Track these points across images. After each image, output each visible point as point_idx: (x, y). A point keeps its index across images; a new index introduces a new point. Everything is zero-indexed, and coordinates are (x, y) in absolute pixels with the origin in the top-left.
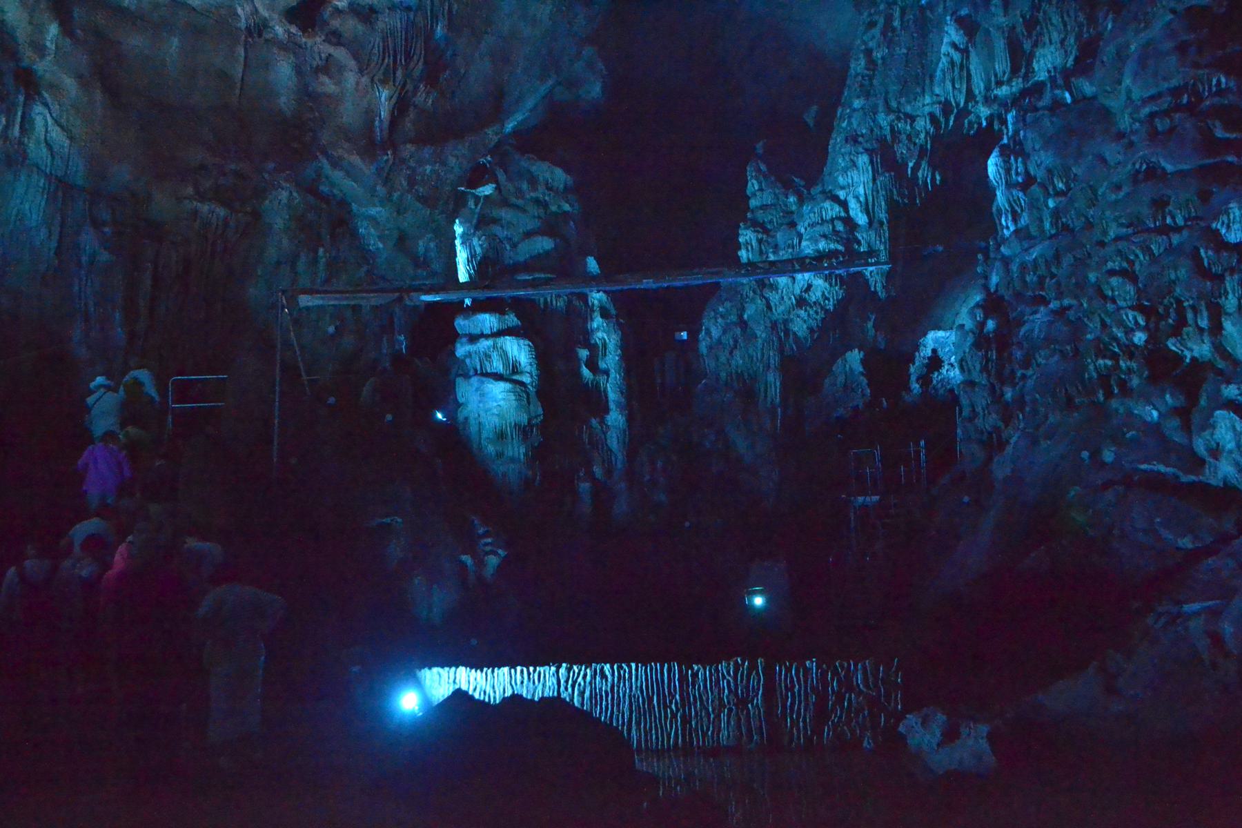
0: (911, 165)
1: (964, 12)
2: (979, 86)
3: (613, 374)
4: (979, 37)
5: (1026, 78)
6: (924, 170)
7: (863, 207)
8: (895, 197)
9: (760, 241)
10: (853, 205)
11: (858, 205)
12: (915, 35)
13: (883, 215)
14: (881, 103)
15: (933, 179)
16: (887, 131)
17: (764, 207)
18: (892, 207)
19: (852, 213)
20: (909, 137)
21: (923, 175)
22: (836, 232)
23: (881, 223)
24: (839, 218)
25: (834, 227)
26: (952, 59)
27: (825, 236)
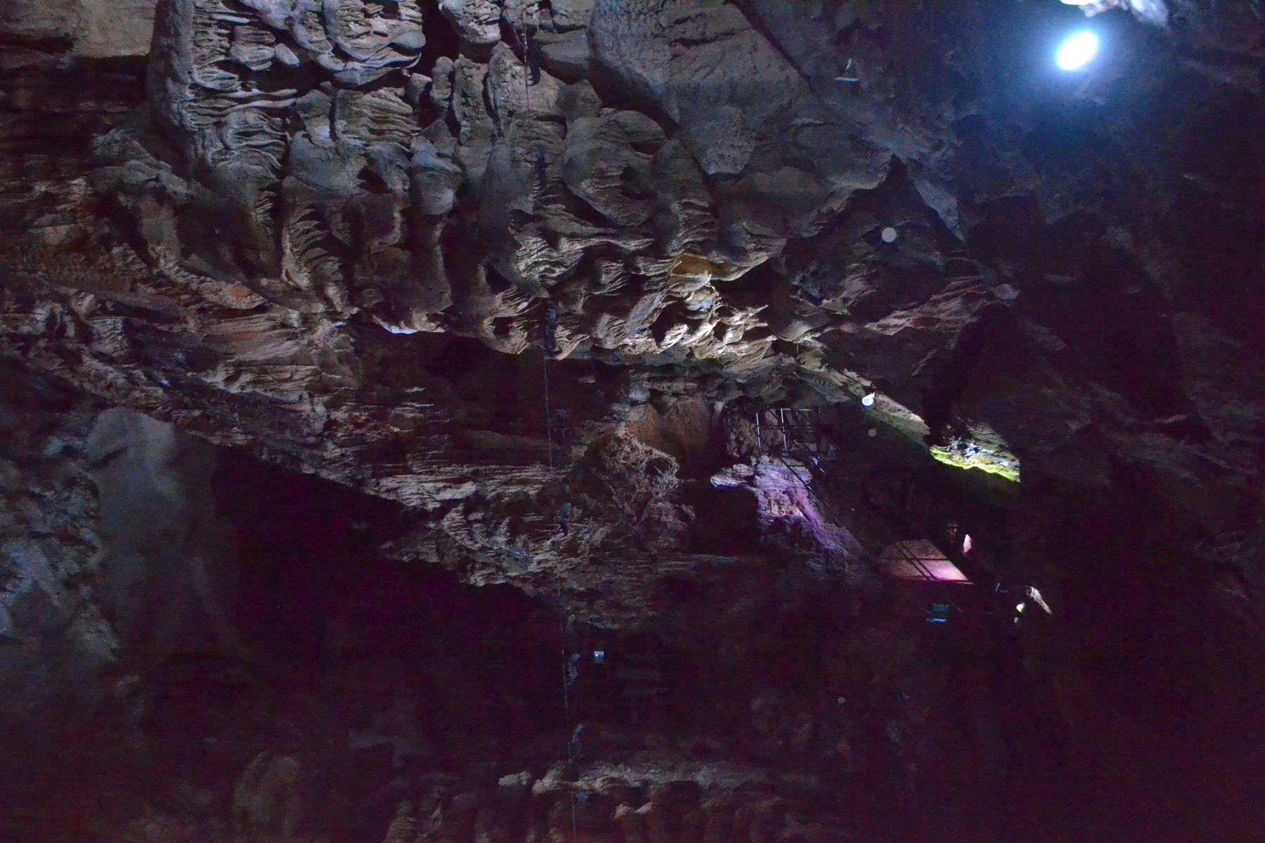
0: (396, 430)
2: (287, 348)
3: (649, 776)
6: (404, 410)
7: (452, 485)
8: (441, 452)
10: (447, 495)
11: (449, 490)
12: (213, 400)
13: (466, 470)
14: (307, 452)
15: (415, 397)
16: (350, 450)
19: (458, 496)
20: (358, 426)
21: (412, 412)
22: (483, 521)
24: (466, 513)
25: (477, 521)
26: (249, 383)
27: (489, 534)
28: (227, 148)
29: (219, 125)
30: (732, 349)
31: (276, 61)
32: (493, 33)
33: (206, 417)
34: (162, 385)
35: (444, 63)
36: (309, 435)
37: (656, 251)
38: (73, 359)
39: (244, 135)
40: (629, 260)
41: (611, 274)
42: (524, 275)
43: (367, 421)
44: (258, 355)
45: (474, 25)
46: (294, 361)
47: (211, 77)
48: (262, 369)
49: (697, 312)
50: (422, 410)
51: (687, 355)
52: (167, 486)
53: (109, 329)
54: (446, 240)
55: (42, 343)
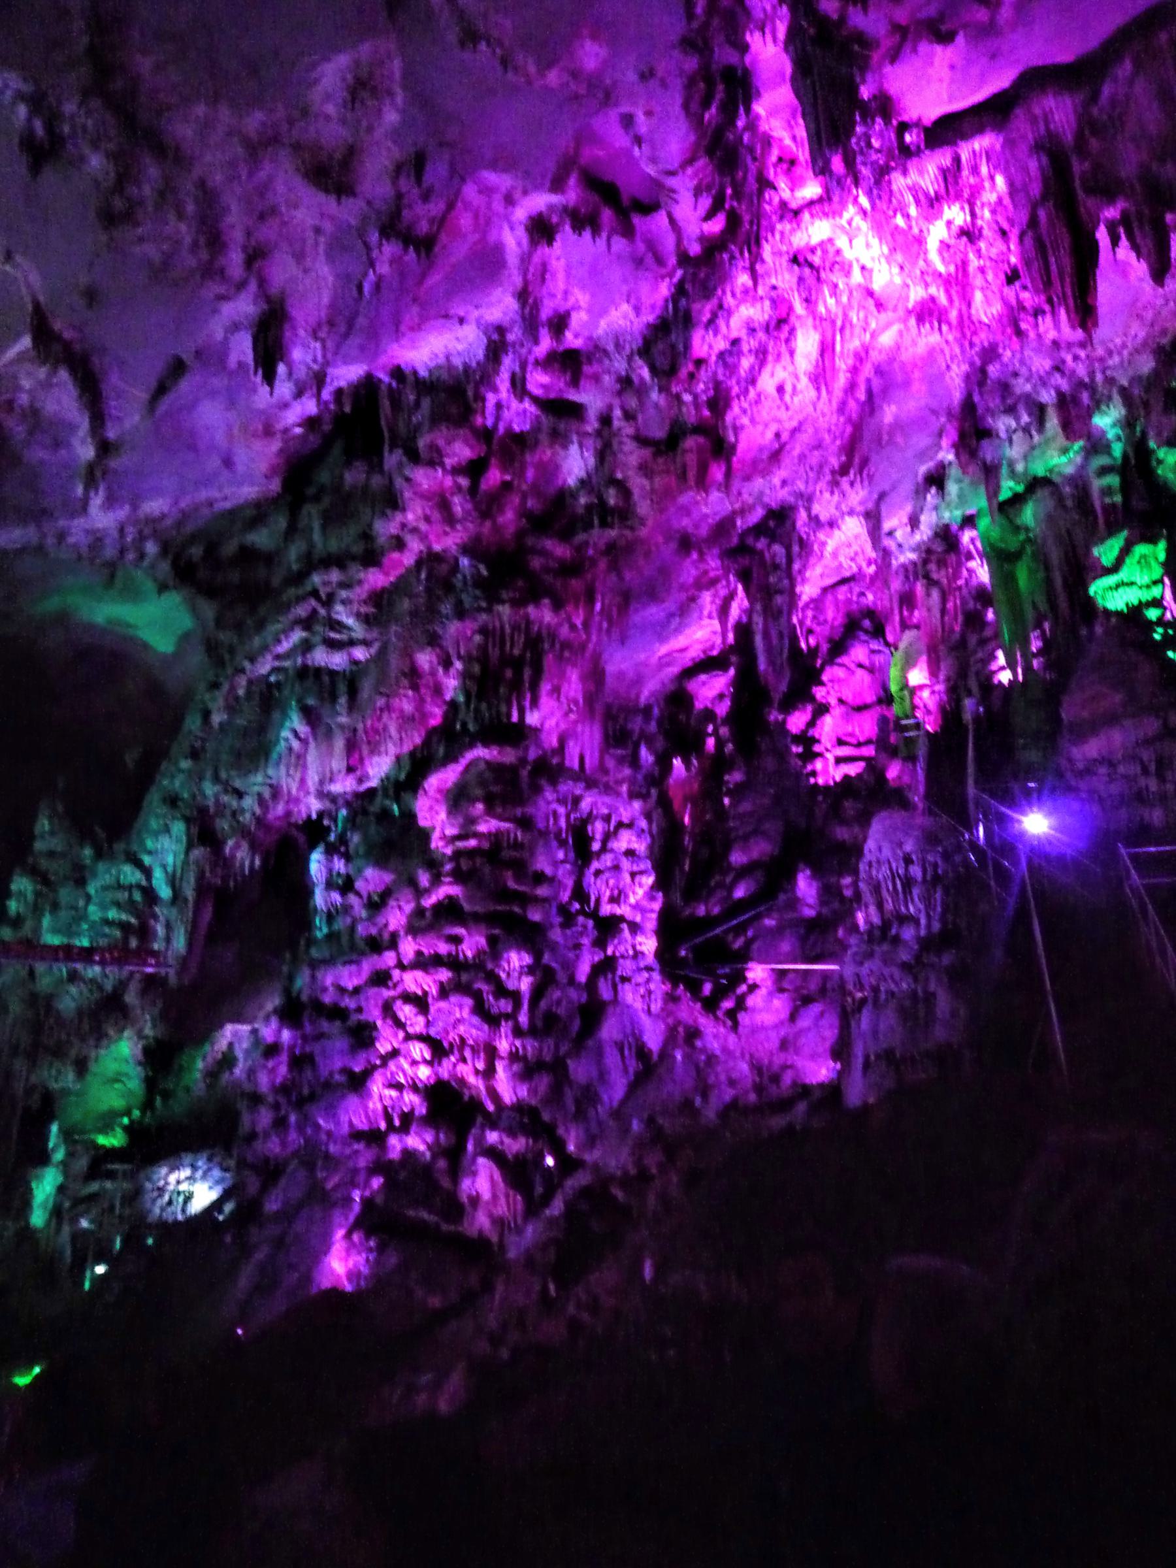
1: (311, 702)
2: (313, 779)
4: (322, 730)
5: (360, 781)
9: (38, 894)
13: (189, 893)
17: (51, 854)
18: (202, 889)
19: (154, 882)
22: (131, 901)
23: (186, 900)
24: (139, 886)
25: (131, 895)
27: (118, 905)
28: (549, 803)
29: (558, 801)
30: (376, 1097)
31: (592, 839)
32: (610, 952)
33: (237, 698)
34: (269, 674)
35: (591, 923)
36: (229, 775)
37: (517, 1032)
38: (307, 623)
39: (555, 813)
40: (512, 1017)
41: (505, 1005)
42: (505, 955)
43: (238, 822)
44: (312, 757)
45: (616, 941)
46: (303, 781)
47: (585, 805)
48: (301, 758)
49: (440, 1064)
50: (242, 865)
51: (347, 1072)
52: (52, 604)
53: (337, 660)
54: (511, 912)
55: (322, 612)
